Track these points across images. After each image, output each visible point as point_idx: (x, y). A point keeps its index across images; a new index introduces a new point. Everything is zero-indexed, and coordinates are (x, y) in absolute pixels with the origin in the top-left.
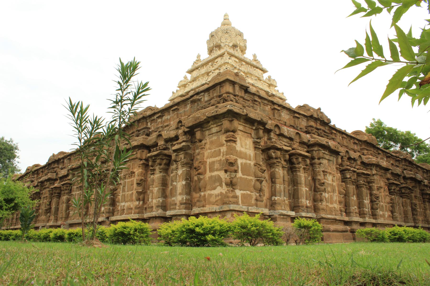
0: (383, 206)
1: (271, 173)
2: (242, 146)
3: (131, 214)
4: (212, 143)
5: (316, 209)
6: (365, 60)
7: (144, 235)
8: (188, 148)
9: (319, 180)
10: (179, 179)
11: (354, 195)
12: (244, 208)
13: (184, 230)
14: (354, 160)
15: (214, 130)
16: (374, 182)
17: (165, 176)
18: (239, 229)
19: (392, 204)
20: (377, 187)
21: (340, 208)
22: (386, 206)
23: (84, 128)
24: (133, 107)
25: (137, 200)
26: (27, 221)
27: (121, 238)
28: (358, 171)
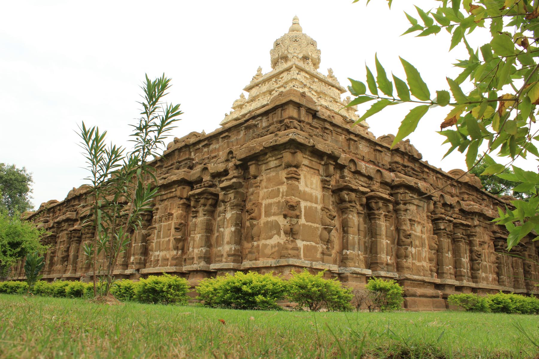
0: (486, 266)
1: (342, 220)
2: (306, 186)
3: (167, 266)
4: (269, 180)
5: (399, 268)
6: (368, 99)
7: (180, 293)
8: (240, 185)
9: (405, 230)
10: (228, 225)
11: (449, 250)
12: (307, 263)
13: (228, 288)
14: (451, 206)
15: (273, 163)
16: (475, 235)
17: (210, 220)
18: (297, 289)
19: (499, 264)
20: (479, 241)
21: (430, 266)
22: (490, 266)
23: (100, 160)
24: (160, 135)
25: (175, 249)
26: (32, 271)
27: (152, 296)
28: (455, 221)
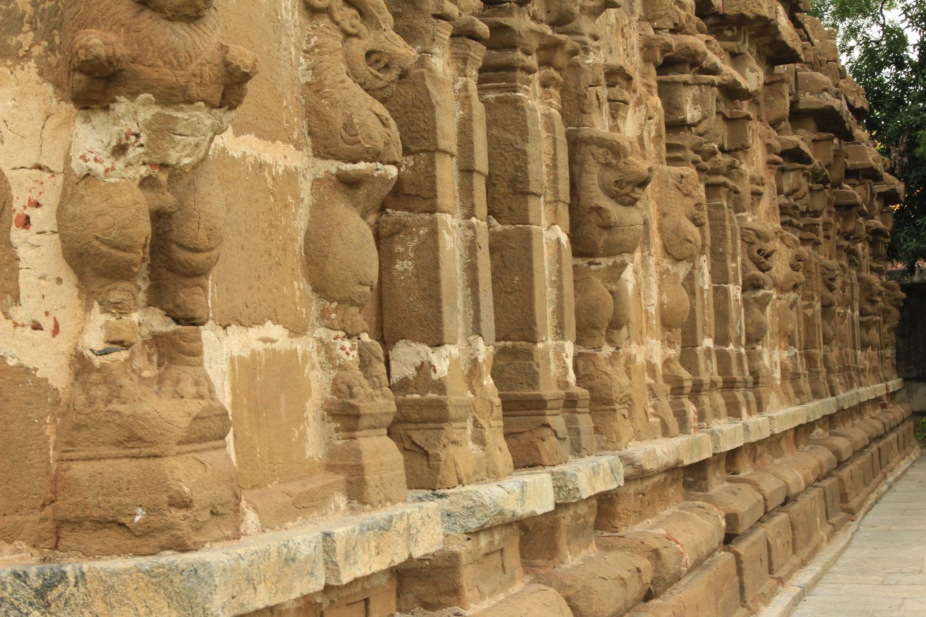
21: (667, 362)
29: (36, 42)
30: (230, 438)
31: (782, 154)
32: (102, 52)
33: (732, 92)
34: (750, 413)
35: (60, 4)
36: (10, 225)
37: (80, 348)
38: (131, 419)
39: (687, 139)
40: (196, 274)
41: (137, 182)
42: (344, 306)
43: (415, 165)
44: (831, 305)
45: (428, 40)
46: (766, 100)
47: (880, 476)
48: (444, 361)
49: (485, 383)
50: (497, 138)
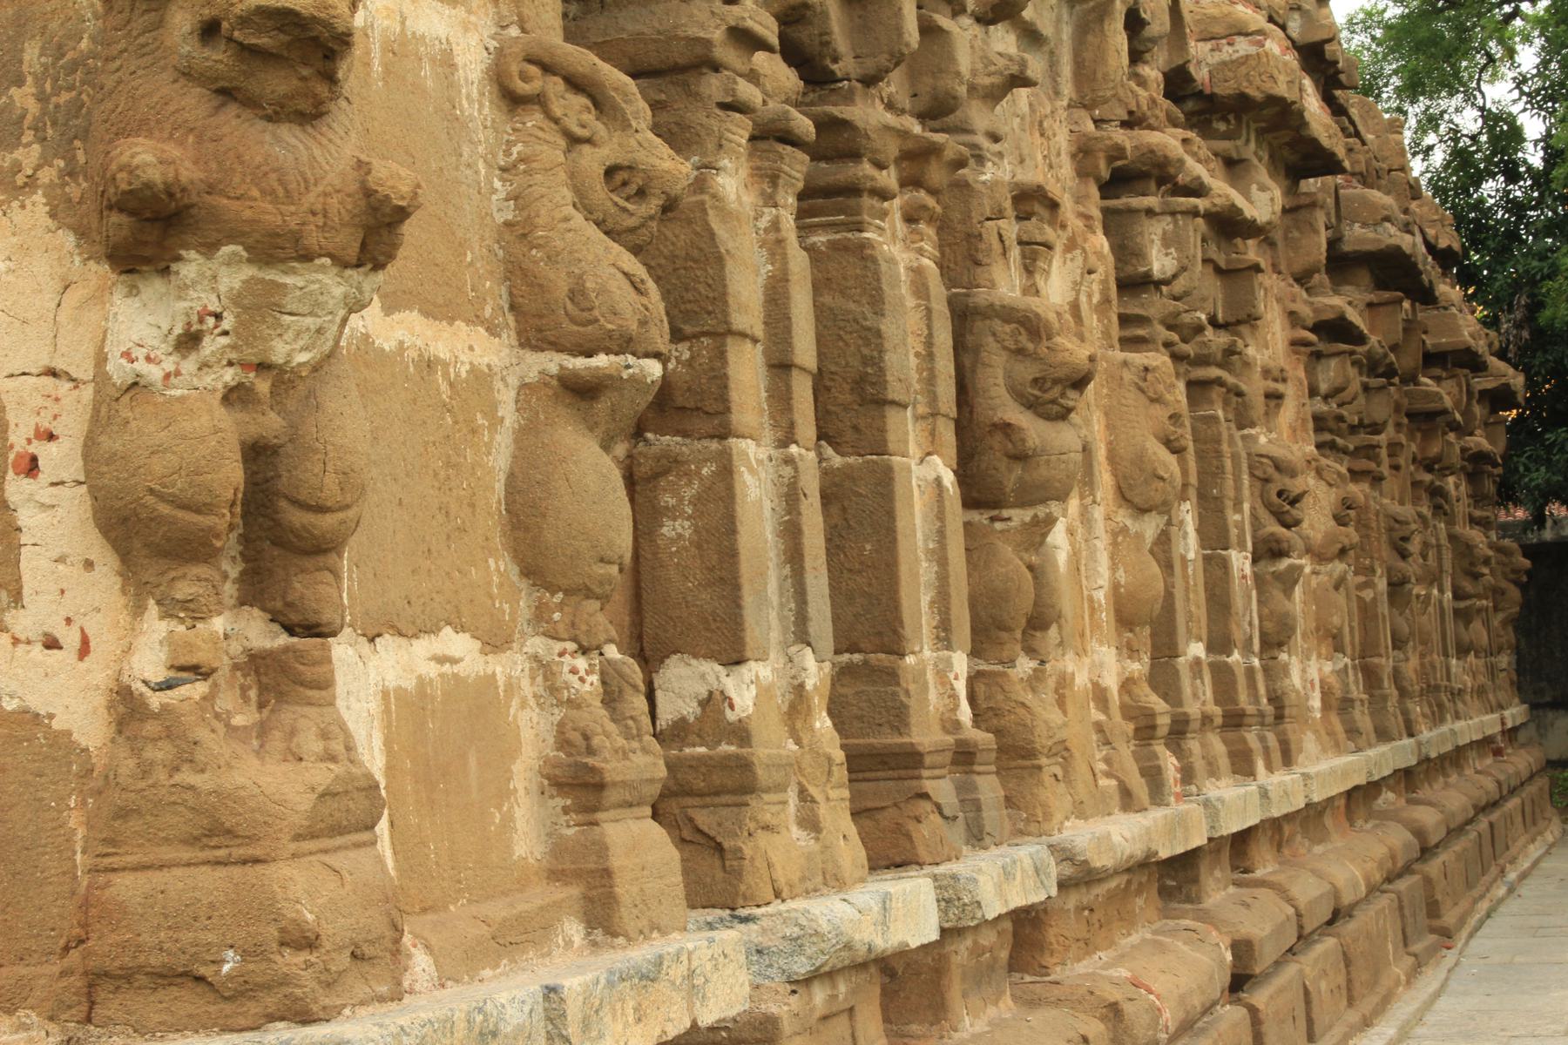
21: (1127, 685)
29: (44, 162)
30: (383, 826)
31: (1316, 328)
32: (155, 175)
33: (1228, 225)
34: (1270, 768)
35: (84, 97)
36: (5, 472)
37: (125, 679)
38: (212, 799)
39: (1154, 305)
40: (320, 549)
41: (219, 395)
42: (574, 599)
43: (692, 357)
44: (1404, 581)
45: (711, 146)
46: (1286, 238)
47: (1494, 870)
48: (747, 690)
49: (818, 725)
50: (831, 309)
